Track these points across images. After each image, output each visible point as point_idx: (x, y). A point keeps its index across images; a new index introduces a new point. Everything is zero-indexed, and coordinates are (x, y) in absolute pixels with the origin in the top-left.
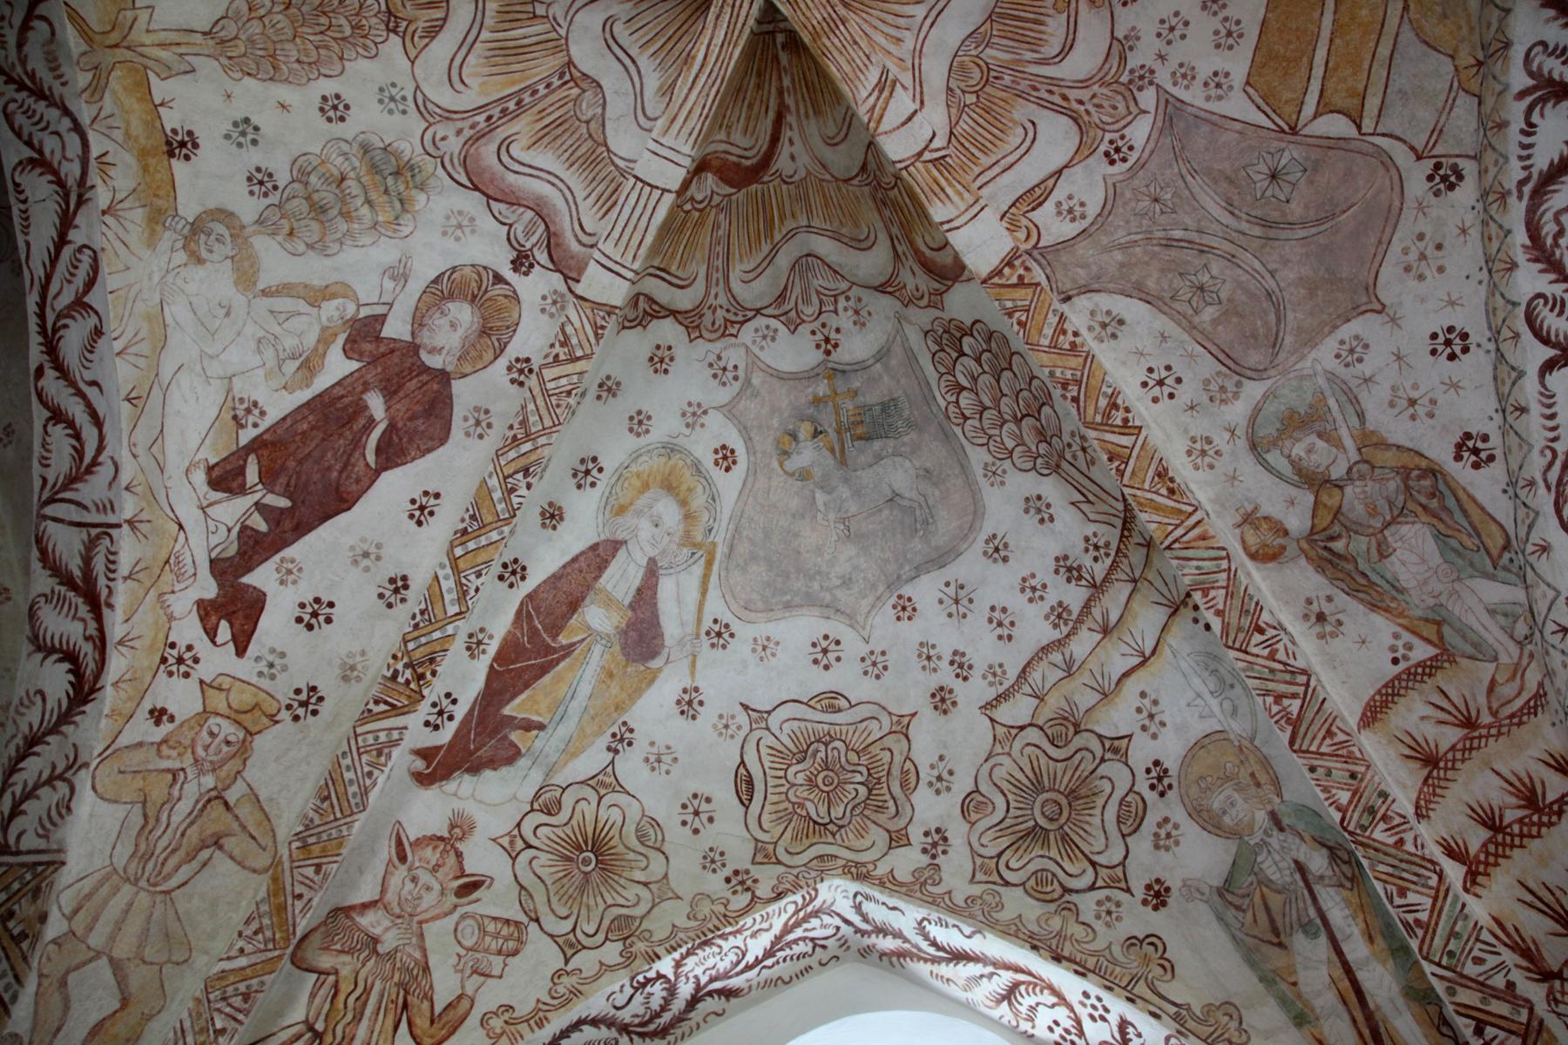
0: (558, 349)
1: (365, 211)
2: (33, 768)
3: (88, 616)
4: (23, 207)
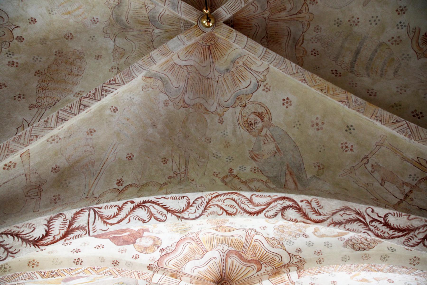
0: (141, 273)
1: (175, 228)
2: (9, 241)
3: (61, 235)
4: (178, 198)
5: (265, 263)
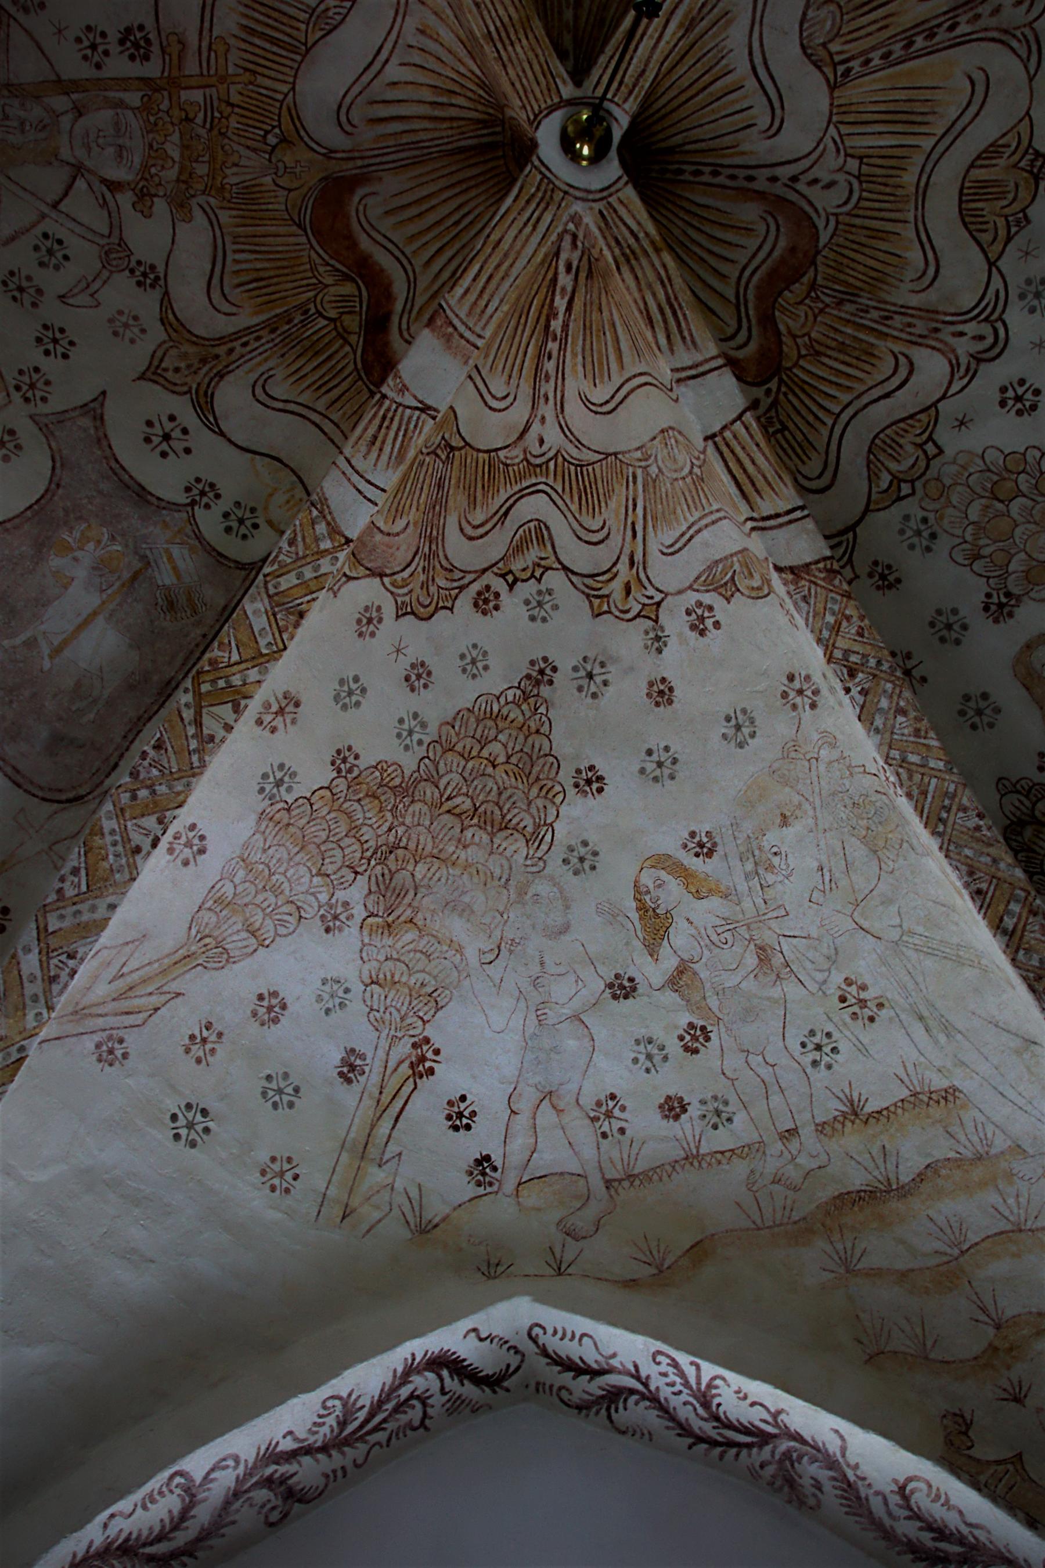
5: (775, 403)
